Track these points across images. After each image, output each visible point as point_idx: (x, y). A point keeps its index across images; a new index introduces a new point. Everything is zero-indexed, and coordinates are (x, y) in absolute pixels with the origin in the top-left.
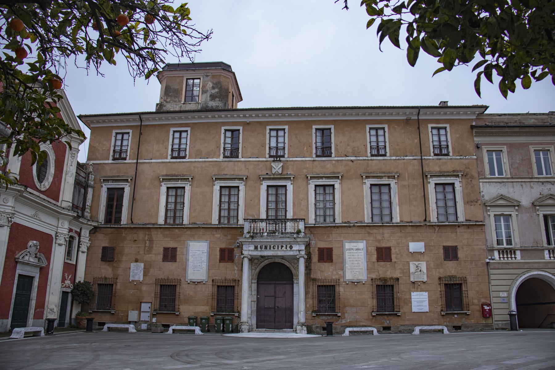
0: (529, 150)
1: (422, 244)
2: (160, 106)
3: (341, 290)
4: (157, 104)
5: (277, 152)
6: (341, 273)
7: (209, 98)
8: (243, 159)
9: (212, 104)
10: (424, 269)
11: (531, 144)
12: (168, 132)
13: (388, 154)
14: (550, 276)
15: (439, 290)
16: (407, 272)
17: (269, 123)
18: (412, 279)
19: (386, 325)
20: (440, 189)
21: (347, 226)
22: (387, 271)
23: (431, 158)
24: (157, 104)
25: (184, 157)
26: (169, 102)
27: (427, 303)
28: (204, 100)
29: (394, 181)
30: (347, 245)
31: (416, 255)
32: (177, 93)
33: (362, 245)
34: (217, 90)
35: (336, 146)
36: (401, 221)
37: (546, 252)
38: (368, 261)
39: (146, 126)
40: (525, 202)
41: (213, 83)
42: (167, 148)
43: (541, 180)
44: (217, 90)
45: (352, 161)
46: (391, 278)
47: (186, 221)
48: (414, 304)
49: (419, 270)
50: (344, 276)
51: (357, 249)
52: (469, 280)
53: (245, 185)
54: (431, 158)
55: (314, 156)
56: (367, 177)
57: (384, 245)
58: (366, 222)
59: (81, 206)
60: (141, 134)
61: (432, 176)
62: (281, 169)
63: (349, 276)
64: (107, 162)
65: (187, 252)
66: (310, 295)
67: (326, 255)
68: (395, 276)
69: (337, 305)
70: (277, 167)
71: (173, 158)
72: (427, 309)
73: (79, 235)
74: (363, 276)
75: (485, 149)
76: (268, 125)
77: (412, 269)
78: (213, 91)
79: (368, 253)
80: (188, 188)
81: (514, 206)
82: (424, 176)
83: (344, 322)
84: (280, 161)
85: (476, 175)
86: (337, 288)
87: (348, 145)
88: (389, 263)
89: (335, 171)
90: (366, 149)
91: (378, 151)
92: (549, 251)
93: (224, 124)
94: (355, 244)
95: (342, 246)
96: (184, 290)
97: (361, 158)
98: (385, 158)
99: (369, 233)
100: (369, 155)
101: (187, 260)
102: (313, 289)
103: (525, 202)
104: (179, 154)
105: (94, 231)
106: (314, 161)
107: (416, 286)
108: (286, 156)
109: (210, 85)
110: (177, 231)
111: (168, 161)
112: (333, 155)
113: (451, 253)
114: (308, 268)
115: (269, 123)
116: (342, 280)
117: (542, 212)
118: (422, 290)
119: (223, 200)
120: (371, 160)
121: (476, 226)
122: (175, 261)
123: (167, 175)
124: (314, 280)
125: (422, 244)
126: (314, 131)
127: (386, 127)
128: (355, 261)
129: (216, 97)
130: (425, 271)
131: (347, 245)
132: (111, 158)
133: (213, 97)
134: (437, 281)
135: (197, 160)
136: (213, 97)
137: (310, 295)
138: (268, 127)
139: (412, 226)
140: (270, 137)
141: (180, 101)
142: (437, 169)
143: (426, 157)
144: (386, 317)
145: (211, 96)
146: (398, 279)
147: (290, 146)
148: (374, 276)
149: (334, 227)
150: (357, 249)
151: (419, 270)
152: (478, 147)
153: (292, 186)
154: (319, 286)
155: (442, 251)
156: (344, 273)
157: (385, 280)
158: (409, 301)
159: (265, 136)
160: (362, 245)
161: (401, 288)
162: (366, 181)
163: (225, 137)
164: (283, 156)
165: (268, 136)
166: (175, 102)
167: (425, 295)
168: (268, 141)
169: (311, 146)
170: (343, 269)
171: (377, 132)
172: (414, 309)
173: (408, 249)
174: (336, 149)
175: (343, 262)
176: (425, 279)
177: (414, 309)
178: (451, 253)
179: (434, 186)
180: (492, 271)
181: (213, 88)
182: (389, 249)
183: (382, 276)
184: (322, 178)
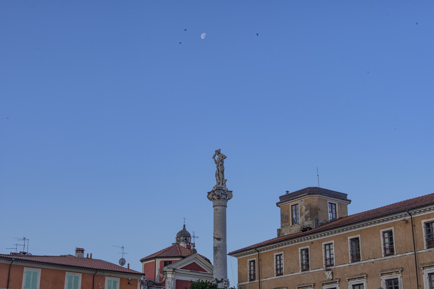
7: (304, 219)
9: (308, 223)
12: (273, 256)
17: (323, 241)
23: (424, 251)
29: (400, 275)
44: (308, 211)
54: (424, 251)
55: (350, 262)
62: (331, 276)
64: (246, 283)
70: (328, 275)
71: (278, 275)
76: (323, 242)
78: (306, 213)
84: (330, 270)
87: (370, 249)
89: (363, 272)
90: (381, 250)
93: (300, 245)
97: (378, 259)
106: (350, 266)
109: (304, 208)
111: (274, 278)
115: (323, 241)
120: (384, 259)
126: (349, 241)
129: (308, 217)
135: (288, 275)
136: (306, 218)
138: (323, 244)
141: (289, 225)
142: (429, 260)
143: (420, 251)
145: (305, 217)
162: (382, 278)
164: (333, 265)
165: (323, 250)
166: (287, 226)
168: (324, 255)
169: (348, 254)
179: (427, 276)
181: (306, 210)
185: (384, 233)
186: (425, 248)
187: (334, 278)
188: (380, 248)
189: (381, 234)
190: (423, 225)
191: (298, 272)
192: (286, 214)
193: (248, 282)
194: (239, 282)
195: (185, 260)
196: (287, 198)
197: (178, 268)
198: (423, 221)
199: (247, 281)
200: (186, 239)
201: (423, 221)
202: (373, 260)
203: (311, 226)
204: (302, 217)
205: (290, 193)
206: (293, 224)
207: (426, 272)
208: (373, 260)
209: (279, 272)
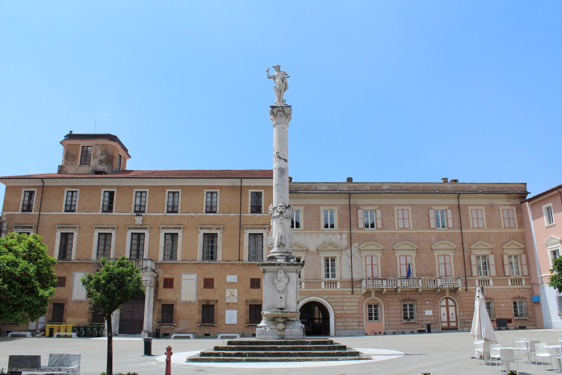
0: (319, 210)
1: (236, 276)
2: (61, 169)
3: (177, 308)
4: (59, 166)
5: (140, 208)
6: (178, 296)
7: (98, 163)
8: (115, 214)
9: (101, 168)
11: (322, 205)
12: (64, 191)
13: (218, 212)
14: (322, 300)
15: (245, 309)
16: (224, 297)
18: (227, 301)
19: (207, 332)
20: (252, 237)
21: (184, 264)
22: (210, 295)
24: (59, 166)
25: (74, 211)
26: (68, 165)
27: (236, 318)
28: (94, 164)
30: (184, 277)
31: (231, 285)
32: (74, 157)
33: (194, 276)
34: (104, 156)
35: (182, 204)
36: (223, 260)
37: (323, 283)
38: (197, 288)
39: (47, 186)
40: (312, 248)
41: (102, 151)
42: (62, 204)
43: (326, 232)
44: (104, 156)
45: (192, 216)
46: (212, 300)
47: (73, 257)
48: (227, 318)
49: (232, 295)
50: (180, 298)
51: (191, 280)
53: (116, 232)
55: (166, 212)
56: (201, 228)
58: (198, 260)
60: (43, 192)
61: (246, 229)
63: (184, 298)
64: (17, 213)
65: (73, 280)
66: (156, 311)
67: (169, 283)
68: (215, 299)
69: (174, 318)
70: (139, 220)
71: (66, 211)
72: (235, 322)
77: (228, 293)
78: (102, 157)
79: (198, 282)
80: (76, 234)
81: (304, 251)
82: (241, 228)
83: (178, 329)
84: (141, 215)
86: (175, 306)
88: (211, 290)
90: (203, 207)
92: (325, 283)
94: (189, 276)
95: (180, 277)
96: (69, 308)
98: (215, 214)
99: (199, 268)
100: (204, 212)
101: (73, 285)
103: (312, 248)
104: (71, 208)
107: (230, 306)
108: (146, 212)
109: (99, 152)
110: (66, 264)
112: (179, 212)
114: (156, 292)
116: (178, 301)
117: (323, 255)
118: (233, 309)
119: (100, 243)
122: (64, 286)
123: (61, 224)
124: (160, 300)
125: (236, 276)
126: (167, 193)
127: (218, 191)
128: (188, 289)
130: (236, 295)
131: (184, 277)
132: (20, 210)
133: (101, 162)
134: (244, 303)
136: (101, 162)
137: (156, 311)
138: (135, 190)
139: (230, 264)
140: (136, 197)
141: (76, 164)
144: (207, 327)
145: (100, 161)
146: (217, 301)
147: (149, 204)
148: (201, 298)
149: (176, 263)
150: (191, 280)
151: (232, 295)
153: (148, 234)
154: (163, 305)
155: (249, 282)
156: (180, 296)
157: (208, 301)
158: (224, 317)
159: (132, 196)
160: (194, 276)
161: (218, 308)
163: (104, 197)
164: (144, 212)
165: (134, 196)
166: (73, 165)
167: (235, 312)
169: (164, 205)
170: (180, 293)
171: (212, 195)
172: (227, 322)
173: (226, 280)
174: (181, 208)
175: (180, 288)
176: (236, 301)
177: (227, 322)
181: (102, 154)
182: (212, 280)
183: (206, 298)
184: (169, 228)
185: (207, 192)
186: (249, 212)
187: (144, 224)
188: (202, 205)
189: (205, 193)
190: (250, 193)
191: (98, 211)
192: (74, 153)
193: (20, 213)
194: (3, 210)
196: (71, 136)
198: (250, 191)
199: (18, 211)
201: (250, 191)
202: (193, 214)
203: (106, 171)
204: (95, 160)
205: (73, 133)
206: (80, 164)
207: (248, 232)
208: (193, 214)
209: (70, 208)
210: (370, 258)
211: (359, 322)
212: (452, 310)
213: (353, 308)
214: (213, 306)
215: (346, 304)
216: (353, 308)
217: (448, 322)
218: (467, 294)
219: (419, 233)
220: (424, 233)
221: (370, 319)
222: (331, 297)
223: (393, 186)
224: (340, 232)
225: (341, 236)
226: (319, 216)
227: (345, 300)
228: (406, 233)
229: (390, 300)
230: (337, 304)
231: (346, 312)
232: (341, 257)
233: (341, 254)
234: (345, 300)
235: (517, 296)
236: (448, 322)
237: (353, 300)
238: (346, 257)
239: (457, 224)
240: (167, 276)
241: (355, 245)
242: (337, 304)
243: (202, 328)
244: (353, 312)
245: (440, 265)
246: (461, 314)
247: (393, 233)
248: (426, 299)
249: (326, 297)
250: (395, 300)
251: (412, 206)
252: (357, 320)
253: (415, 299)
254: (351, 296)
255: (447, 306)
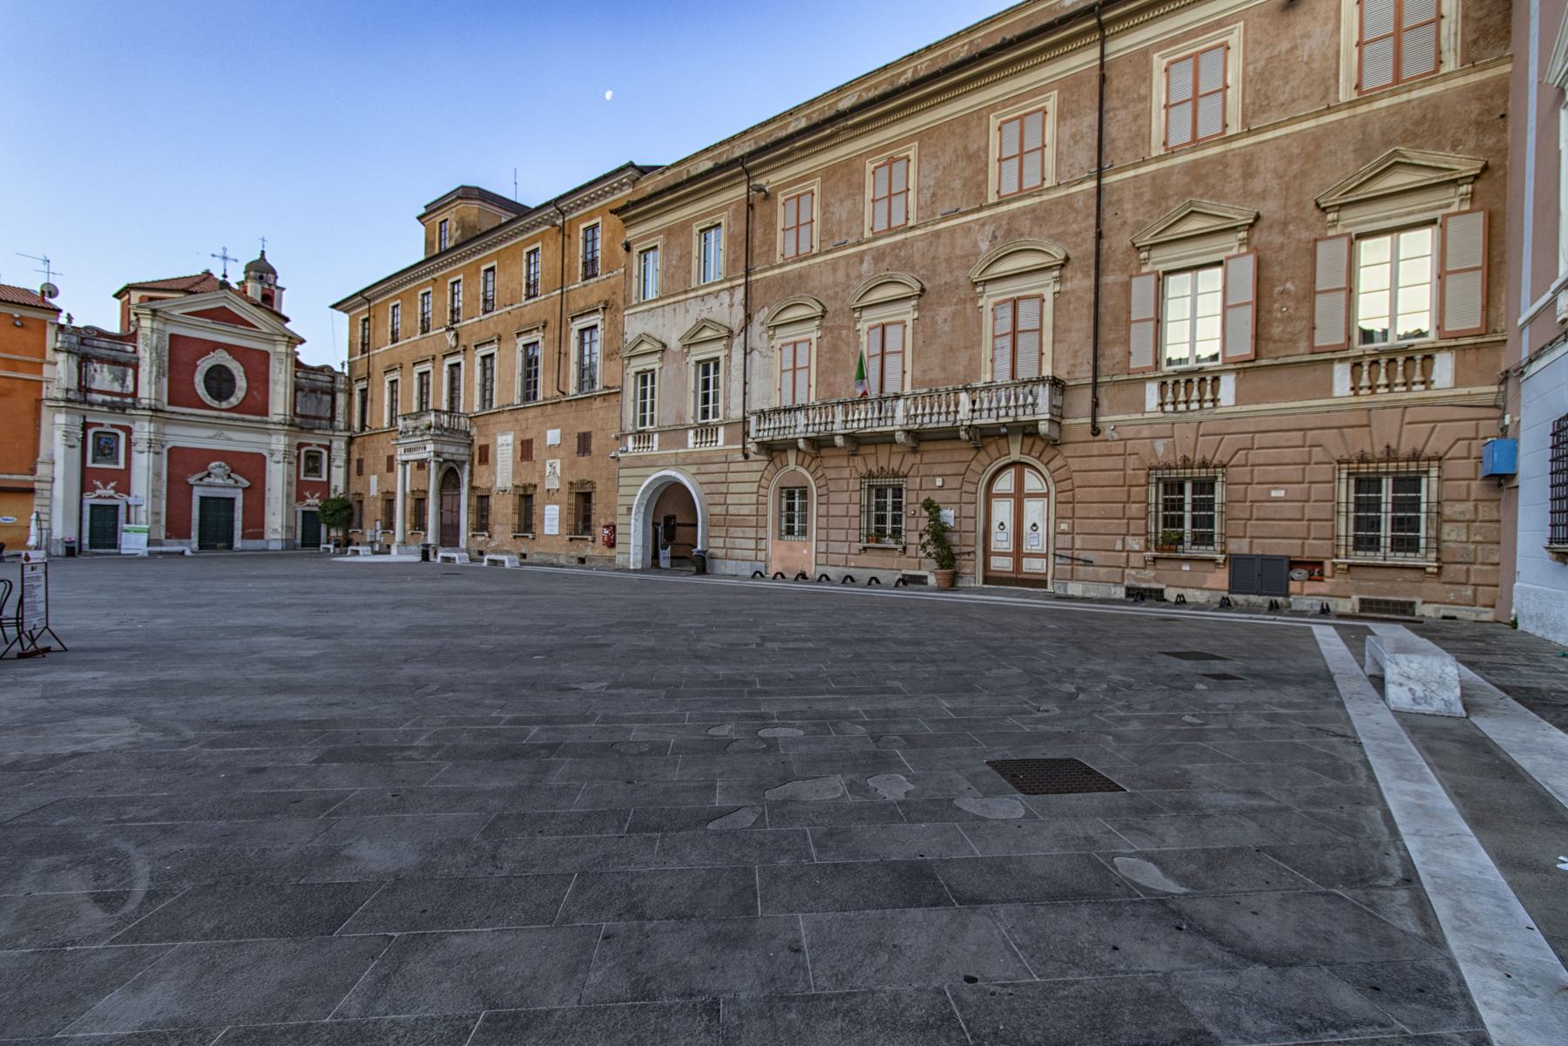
10: (558, 470)
30: (501, 439)
33: (509, 438)
50: (494, 483)
52: (599, 488)
56: (518, 335)
57: (528, 437)
59: (328, 414)
63: (499, 484)
67: (485, 455)
72: (556, 532)
73: (329, 448)
74: (509, 485)
75: (636, 250)
85: (620, 302)
91: (531, 290)
93: (420, 286)
102: (474, 501)
105: (350, 441)
113: (584, 443)
121: (613, 394)
142: (582, 304)
148: (517, 483)
152: (628, 248)
160: (509, 438)
161: (537, 499)
167: (557, 507)
175: (495, 464)
178: (584, 443)
180: (623, 472)
195: (192, 298)
197: (176, 312)
200: (261, 278)
210: (791, 348)
211: (758, 539)
212: (1035, 511)
213: (746, 499)
214: (531, 496)
215: (734, 488)
216: (746, 499)
217: (1018, 554)
218: (1096, 448)
219: (937, 234)
220: (952, 230)
221: (790, 531)
222: (704, 468)
223: (868, 89)
224: (728, 285)
225: (732, 296)
226: (690, 253)
227: (731, 477)
228: (894, 246)
229: (831, 474)
230: (713, 488)
231: (732, 510)
232: (728, 357)
233: (729, 347)
234: (731, 477)
235: (1379, 450)
236: (1018, 554)
237: (746, 477)
238: (738, 356)
239: (1085, 157)
240: (483, 442)
241: (761, 316)
242: (713, 488)
243: (519, 541)
244: (745, 510)
245: (997, 341)
246: (1064, 527)
247: (856, 254)
248: (937, 469)
249: (694, 469)
250: (846, 473)
251: (922, 136)
252: (751, 533)
253: (904, 469)
254: (742, 466)
255: (1019, 496)
